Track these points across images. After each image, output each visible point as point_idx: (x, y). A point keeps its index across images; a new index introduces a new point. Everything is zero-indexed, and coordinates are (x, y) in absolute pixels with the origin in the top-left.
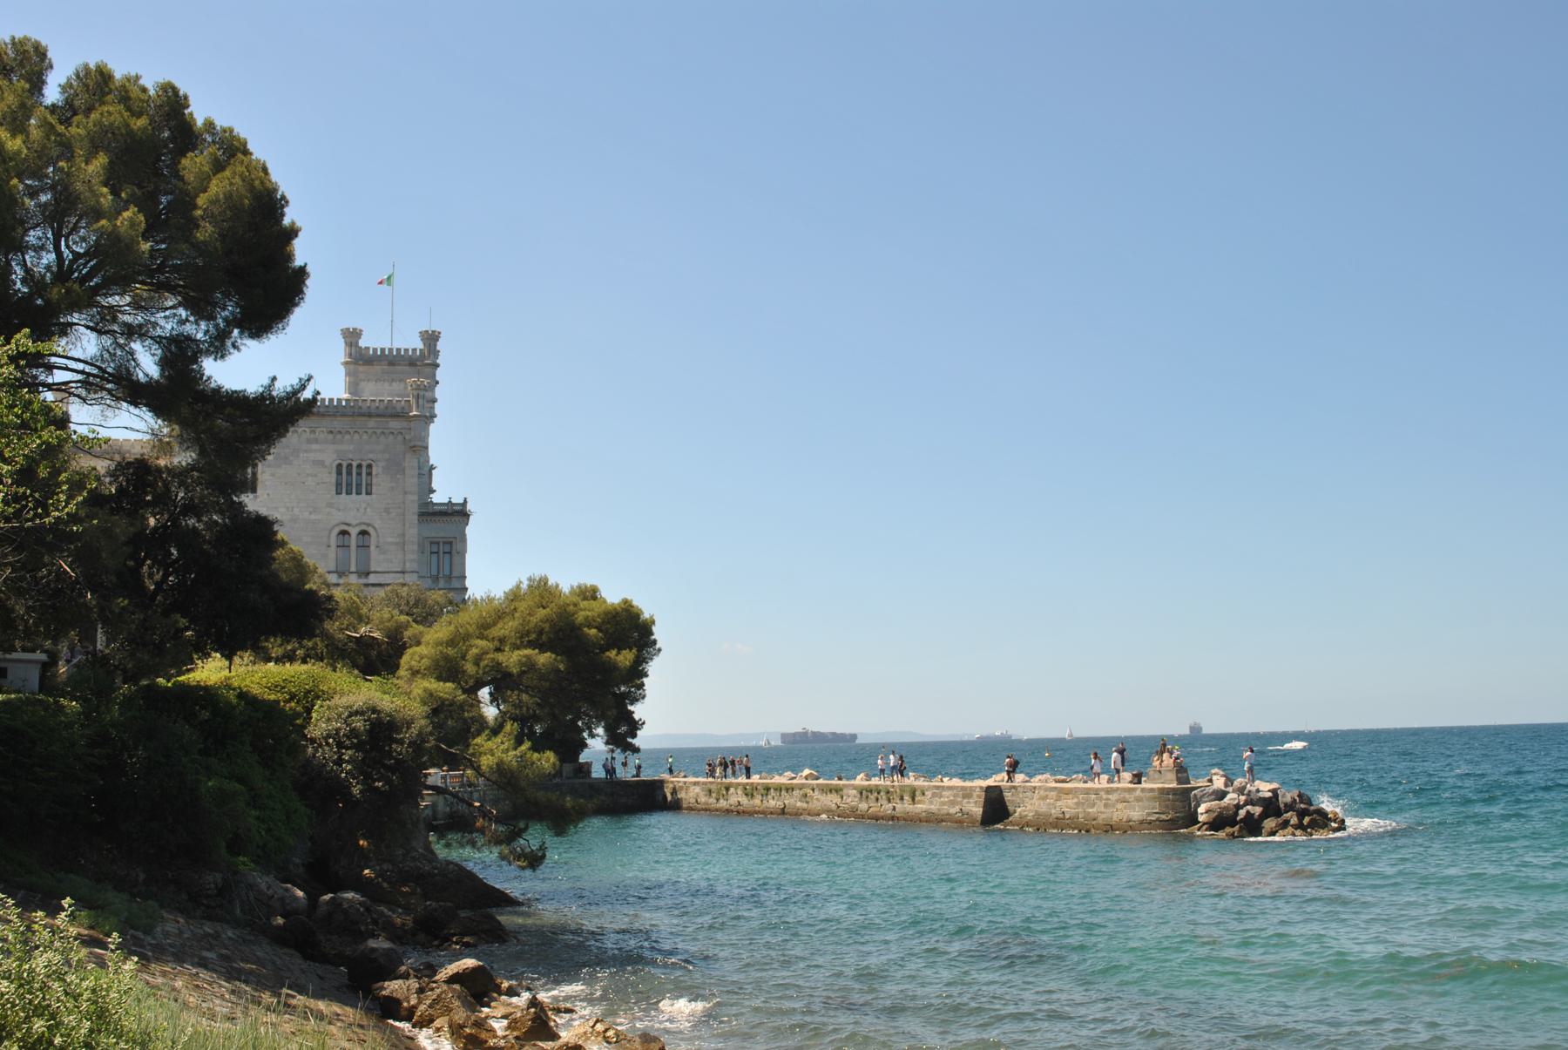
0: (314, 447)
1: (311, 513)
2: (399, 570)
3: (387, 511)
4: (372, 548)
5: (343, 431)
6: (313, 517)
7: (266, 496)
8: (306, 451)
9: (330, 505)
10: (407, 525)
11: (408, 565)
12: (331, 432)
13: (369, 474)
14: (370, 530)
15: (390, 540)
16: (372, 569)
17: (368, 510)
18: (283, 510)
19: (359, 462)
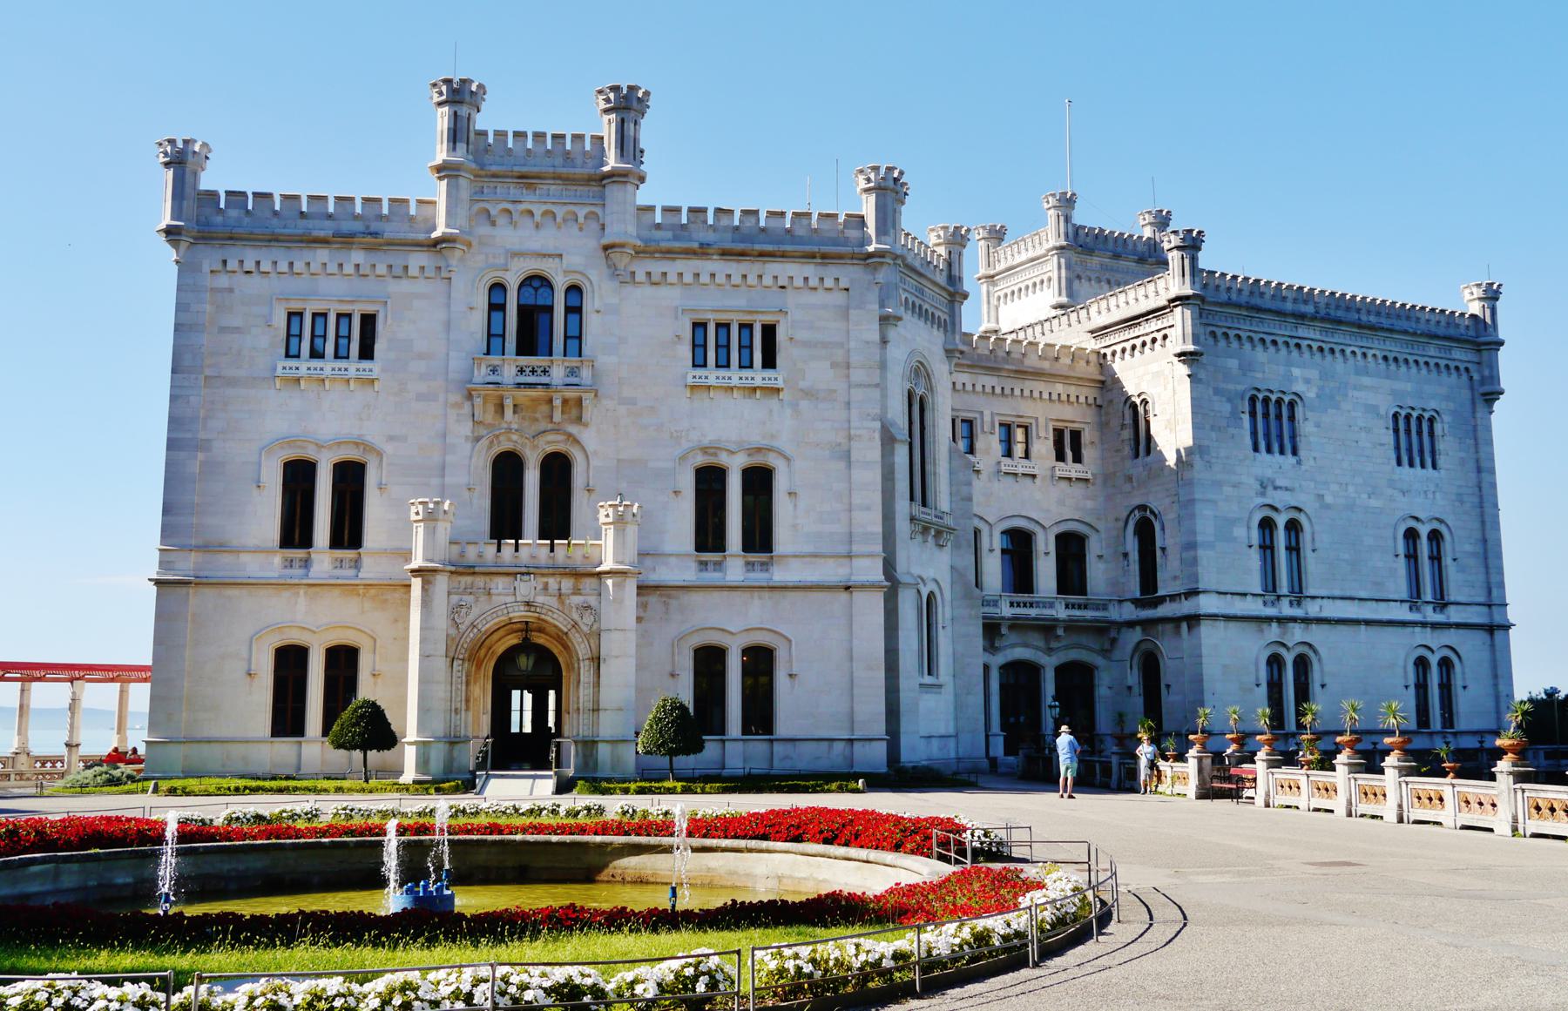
0: (1366, 381)
1: (1369, 498)
2: (1482, 599)
4: (1447, 561)
5: (1401, 358)
6: (1374, 503)
7: (1312, 462)
8: (1355, 388)
9: (1391, 483)
11: (1495, 592)
12: (1385, 358)
14: (1443, 529)
15: (1468, 548)
16: (1452, 599)
17: (1438, 495)
18: (1335, 487)
19: (1421, 412)
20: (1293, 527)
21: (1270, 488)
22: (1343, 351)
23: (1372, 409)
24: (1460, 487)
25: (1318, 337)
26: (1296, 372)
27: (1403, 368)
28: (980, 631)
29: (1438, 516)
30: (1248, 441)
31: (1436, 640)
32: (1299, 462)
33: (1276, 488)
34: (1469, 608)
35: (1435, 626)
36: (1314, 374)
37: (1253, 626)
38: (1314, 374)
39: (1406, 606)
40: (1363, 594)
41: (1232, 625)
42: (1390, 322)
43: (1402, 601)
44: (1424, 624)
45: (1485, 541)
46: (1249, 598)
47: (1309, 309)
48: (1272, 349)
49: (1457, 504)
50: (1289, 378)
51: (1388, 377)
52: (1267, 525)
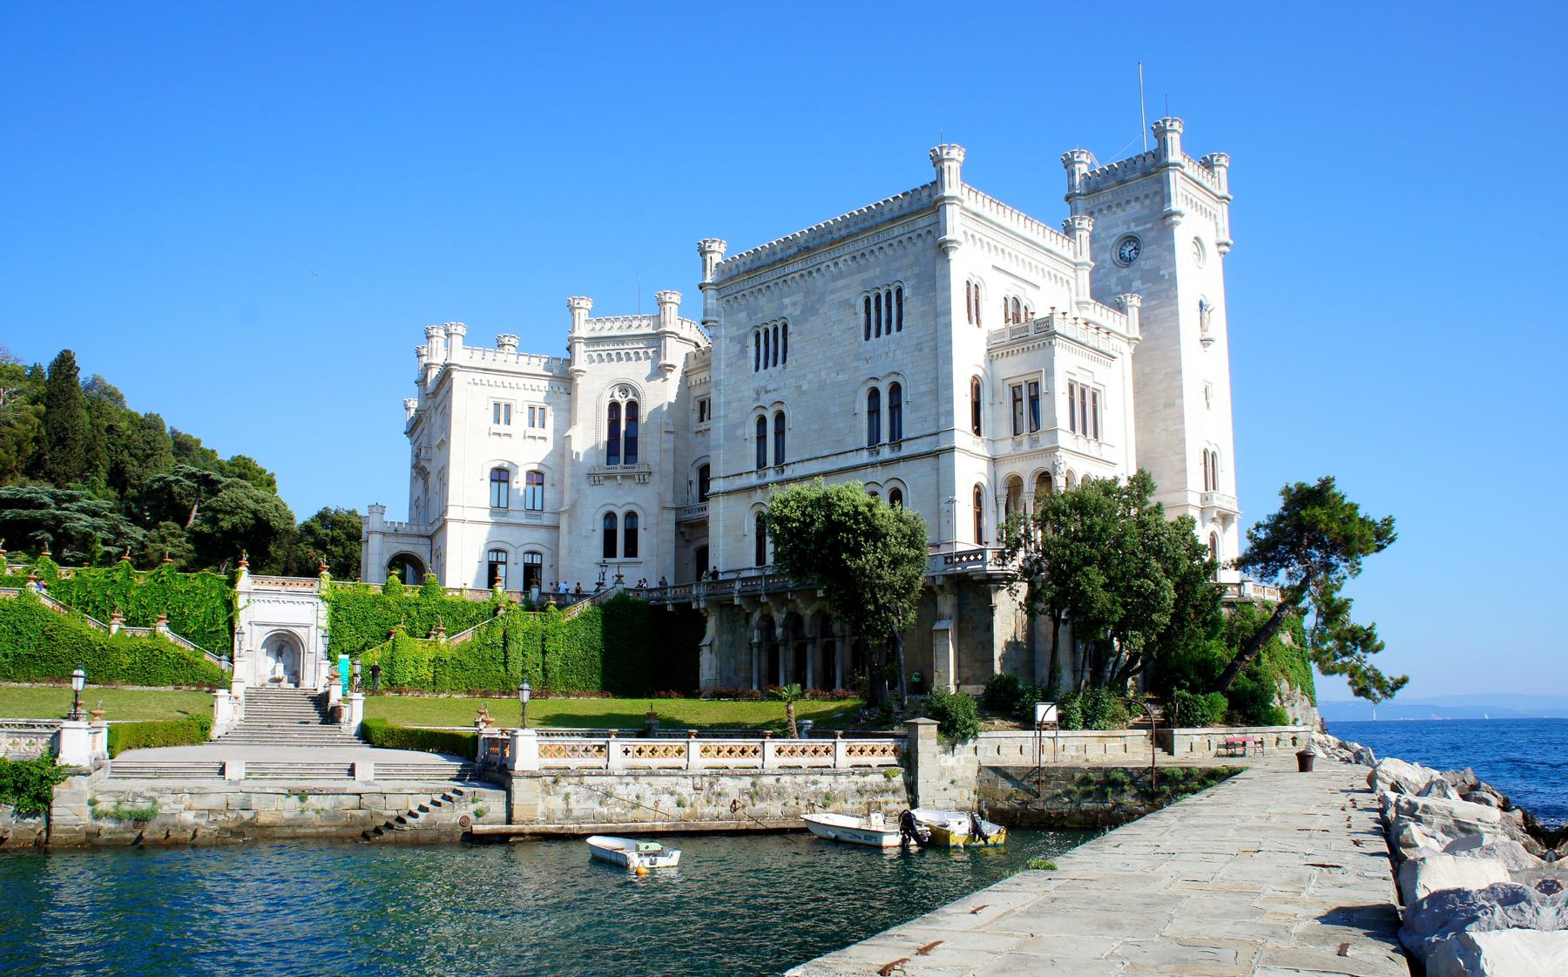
0: (840, 283)
2: (934, 430)
3: (919, 347)
6: (841, 378)
8: (831, 293)
9: (857, 357)
10: (940, 362)
11: (943, 421)
13: (900, 305)
14: (899, 380)
15: (923, 388)
20: (780, 417)
21: (763, 393)
22: (819, 270)
23: (847, 304)
24: (920, 337)
25: (800, 266)
26: (786, 301)
27: (872, 259)
28: (673, 527)
29: (896, 370)
30: (753, 363)
31: (880, 475)
32: (785, 368)
33: (766, 392)
34: (919, 440)
35: (885, 463)
36: (799, 297)
37: (745, 494)
38: (799, 297)
39: (865, 453)
40: (826, 453)
41: (732, 497)
42: (858, 226)
43: (857, 450)
44: (873, 465)
45: (937, 378)
46: (744, 476)
47: (795, 249)
48: (768, 293)
49: (917, 353)
50: (783, 307)
51: (859, 271)
52: (762, 421)
